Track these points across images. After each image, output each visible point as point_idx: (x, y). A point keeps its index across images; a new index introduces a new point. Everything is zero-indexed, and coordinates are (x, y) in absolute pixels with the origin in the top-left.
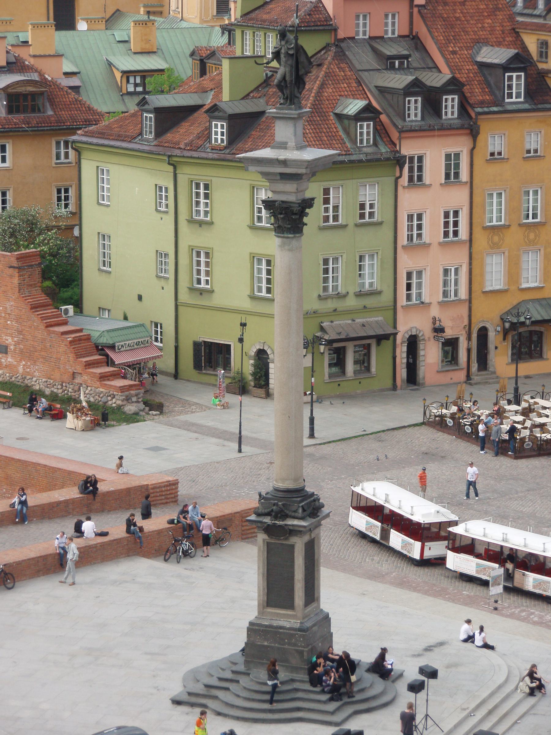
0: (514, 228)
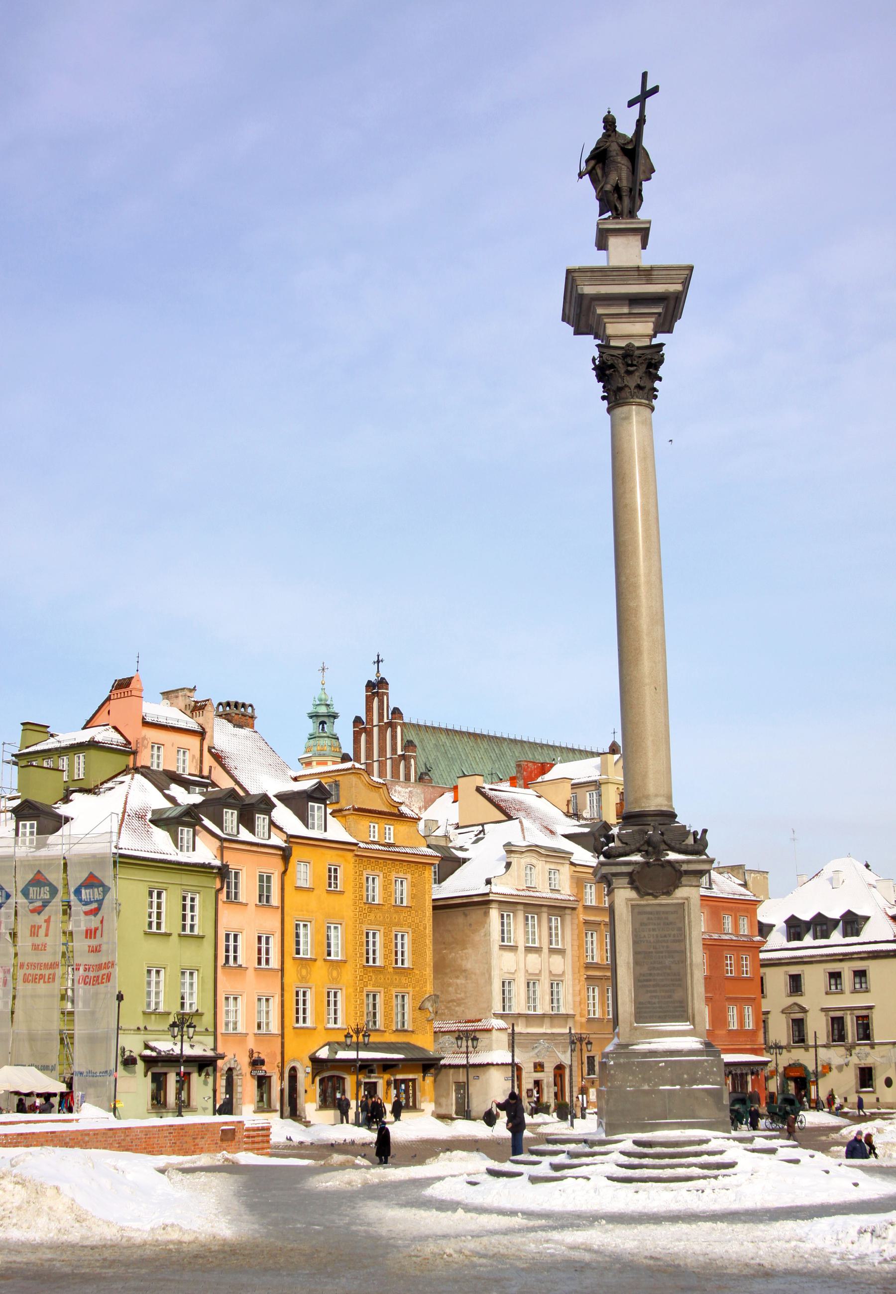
0: (320, 963)
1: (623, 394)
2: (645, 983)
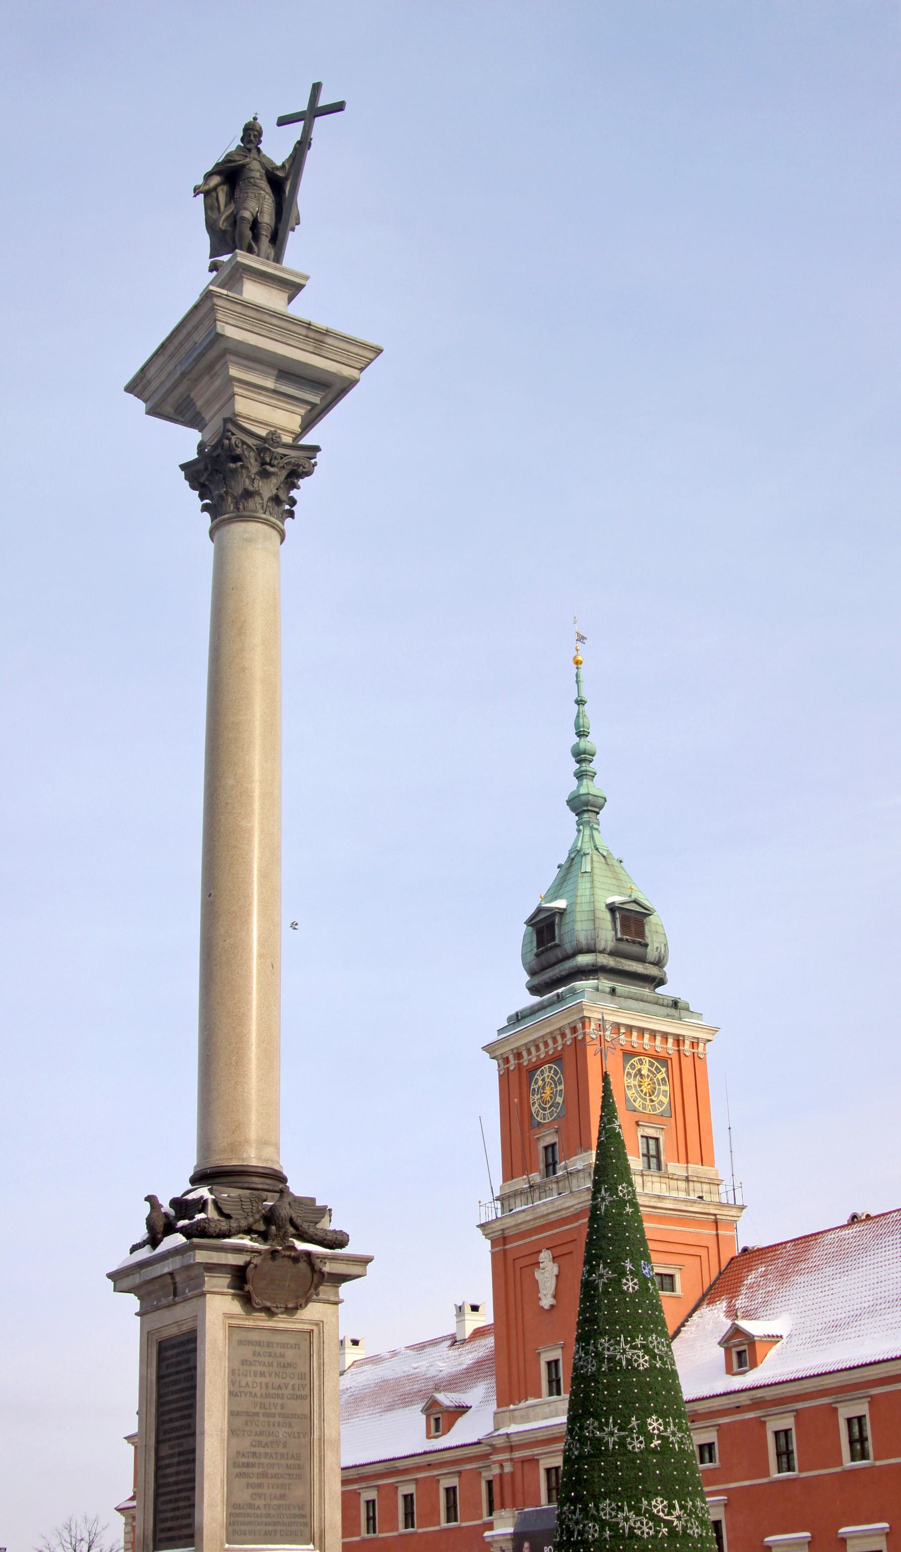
1: (251, 504)
2: (245, 1470)
